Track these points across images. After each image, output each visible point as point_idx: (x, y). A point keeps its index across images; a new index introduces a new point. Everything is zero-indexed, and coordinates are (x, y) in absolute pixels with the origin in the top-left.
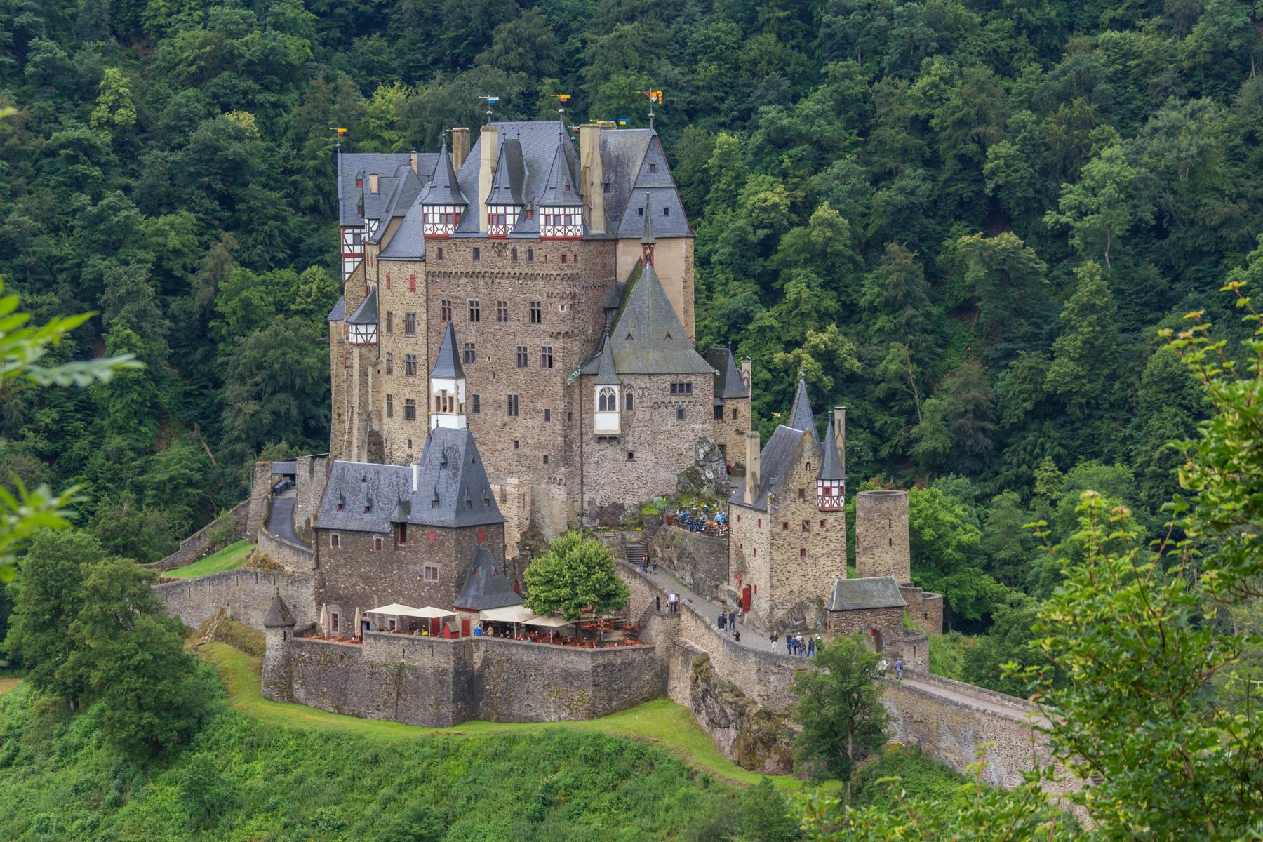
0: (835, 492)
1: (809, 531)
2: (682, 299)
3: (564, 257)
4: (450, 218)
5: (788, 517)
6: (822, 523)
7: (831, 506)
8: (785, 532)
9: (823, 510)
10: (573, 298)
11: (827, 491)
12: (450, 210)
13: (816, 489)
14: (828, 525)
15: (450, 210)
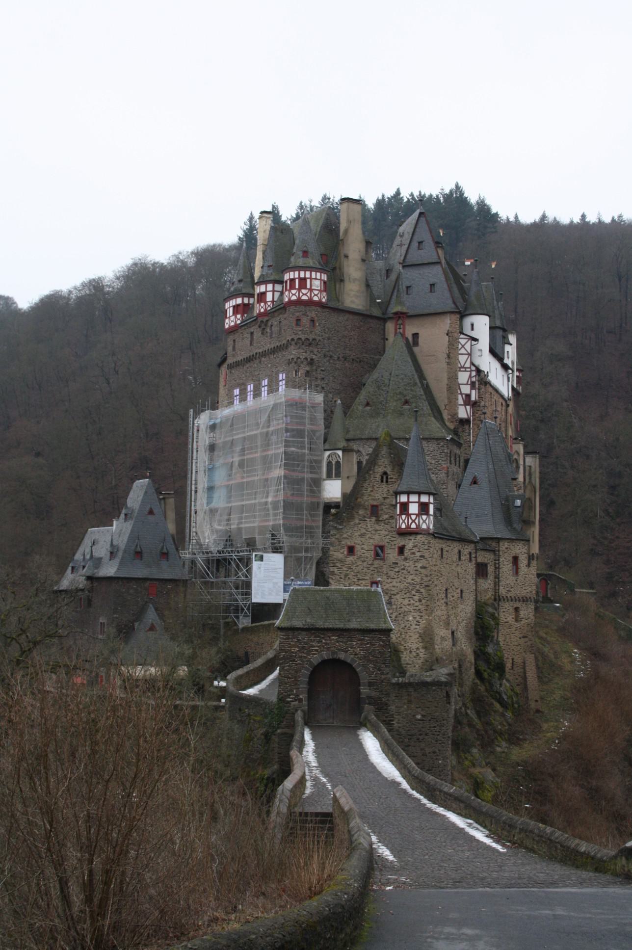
0: (414, 509)
1: (383, 559)
2: (446, 374)
3: (298, 320)
4: (241, 309)
5: (355, 541)
6: (401, 550)
7: (408, 527)
8: (351, 558)
9: (403, 533)
10: (311, 362)
11: (405, 507)
12: (239, 301)
13: (395, 506)
14: (407, 553)
15: (239, 301)
